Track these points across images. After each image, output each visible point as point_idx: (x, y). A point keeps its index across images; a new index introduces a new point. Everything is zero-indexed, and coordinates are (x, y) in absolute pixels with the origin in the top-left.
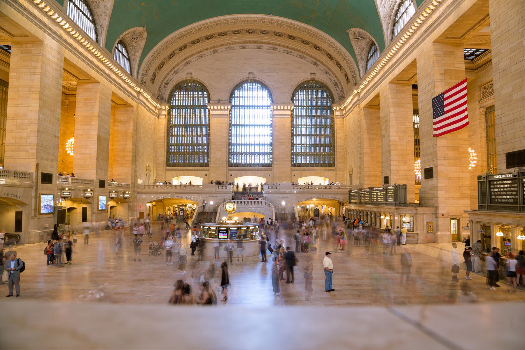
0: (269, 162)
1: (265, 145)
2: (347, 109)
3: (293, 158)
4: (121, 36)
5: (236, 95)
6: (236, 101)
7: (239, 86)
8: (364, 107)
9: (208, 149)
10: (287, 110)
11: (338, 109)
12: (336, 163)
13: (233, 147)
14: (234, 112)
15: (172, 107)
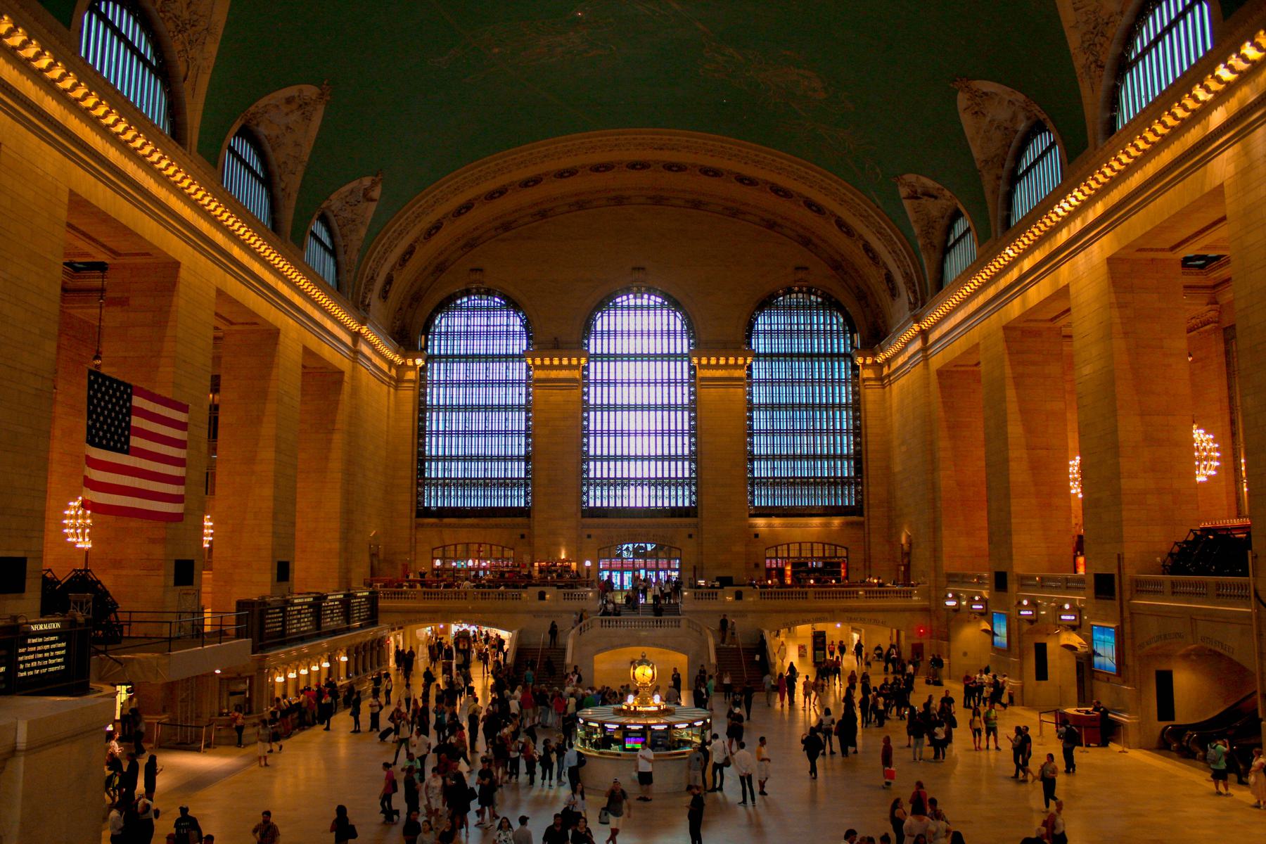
0: (687, 504)
1: (676, 458)
2: (894, 366)
3: (752, 493)
4: (324, 206)
5: (599, 328)
6: (599, 341)
7: (604, 303)
8: (940, 373)
9: (527, 472)
10: (736, 366)
11: (869, 361)
12: (865, 507)
13: (592, 464)
14: (597, 371)
15: (430, 359)
